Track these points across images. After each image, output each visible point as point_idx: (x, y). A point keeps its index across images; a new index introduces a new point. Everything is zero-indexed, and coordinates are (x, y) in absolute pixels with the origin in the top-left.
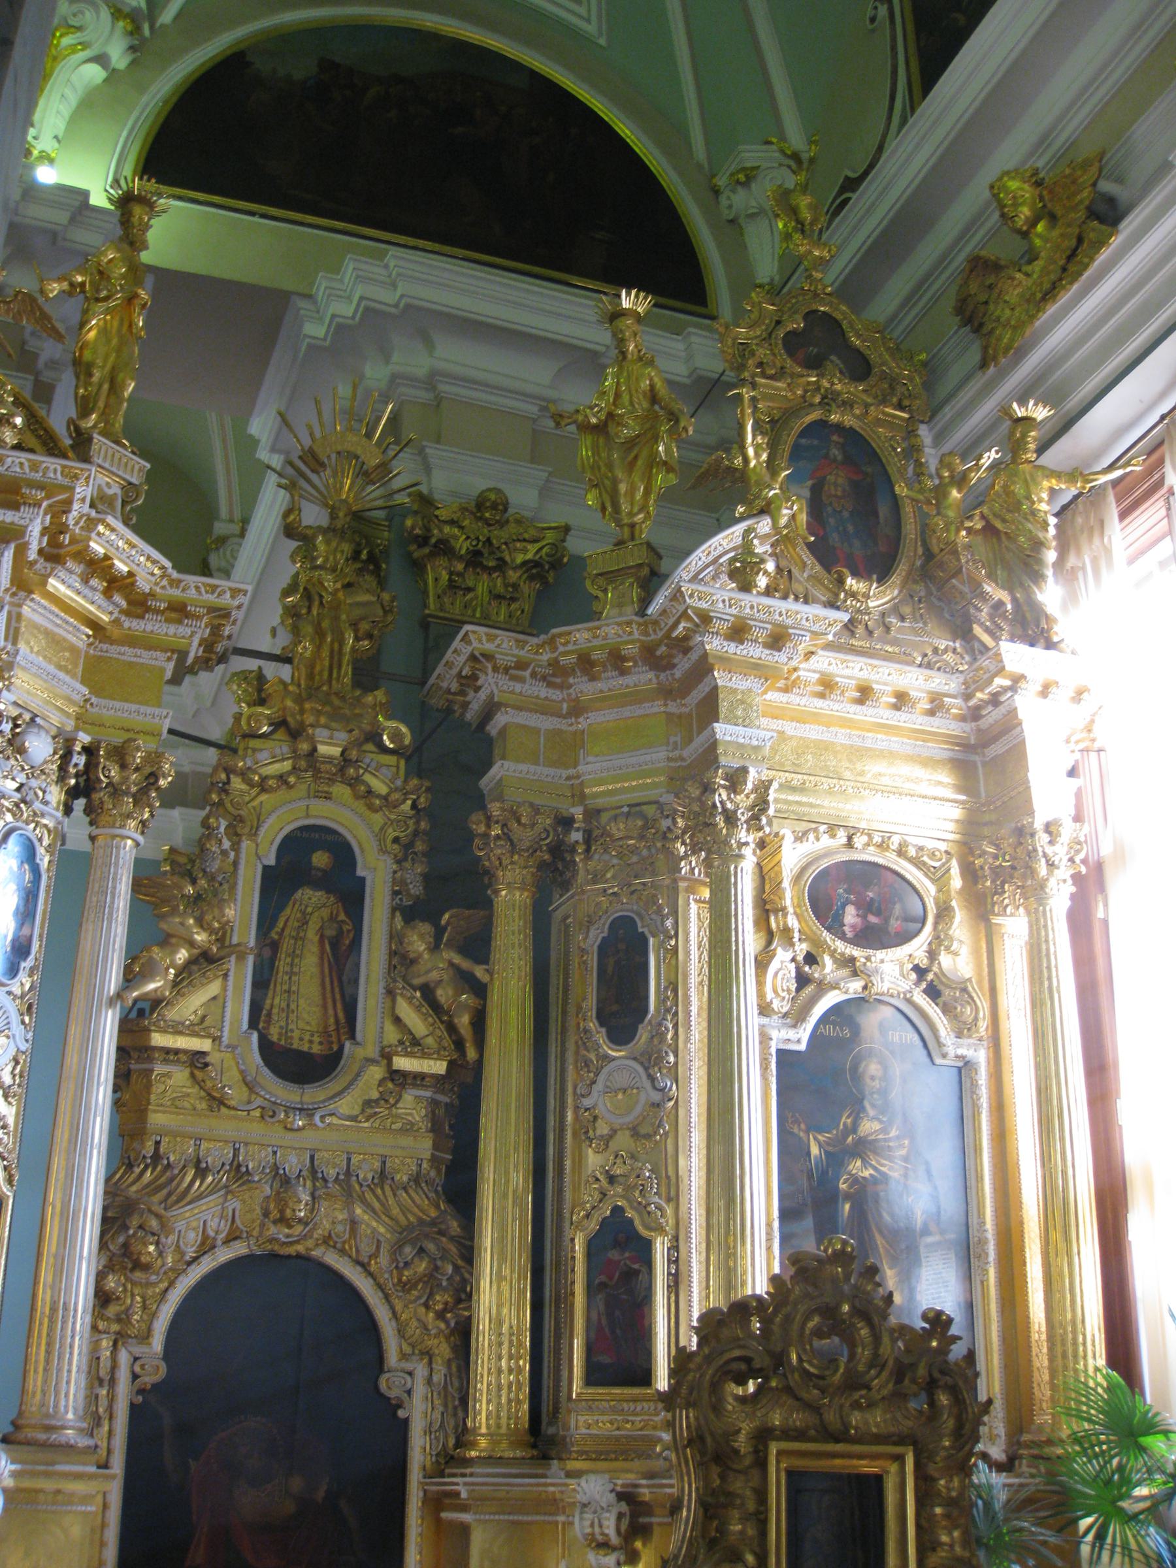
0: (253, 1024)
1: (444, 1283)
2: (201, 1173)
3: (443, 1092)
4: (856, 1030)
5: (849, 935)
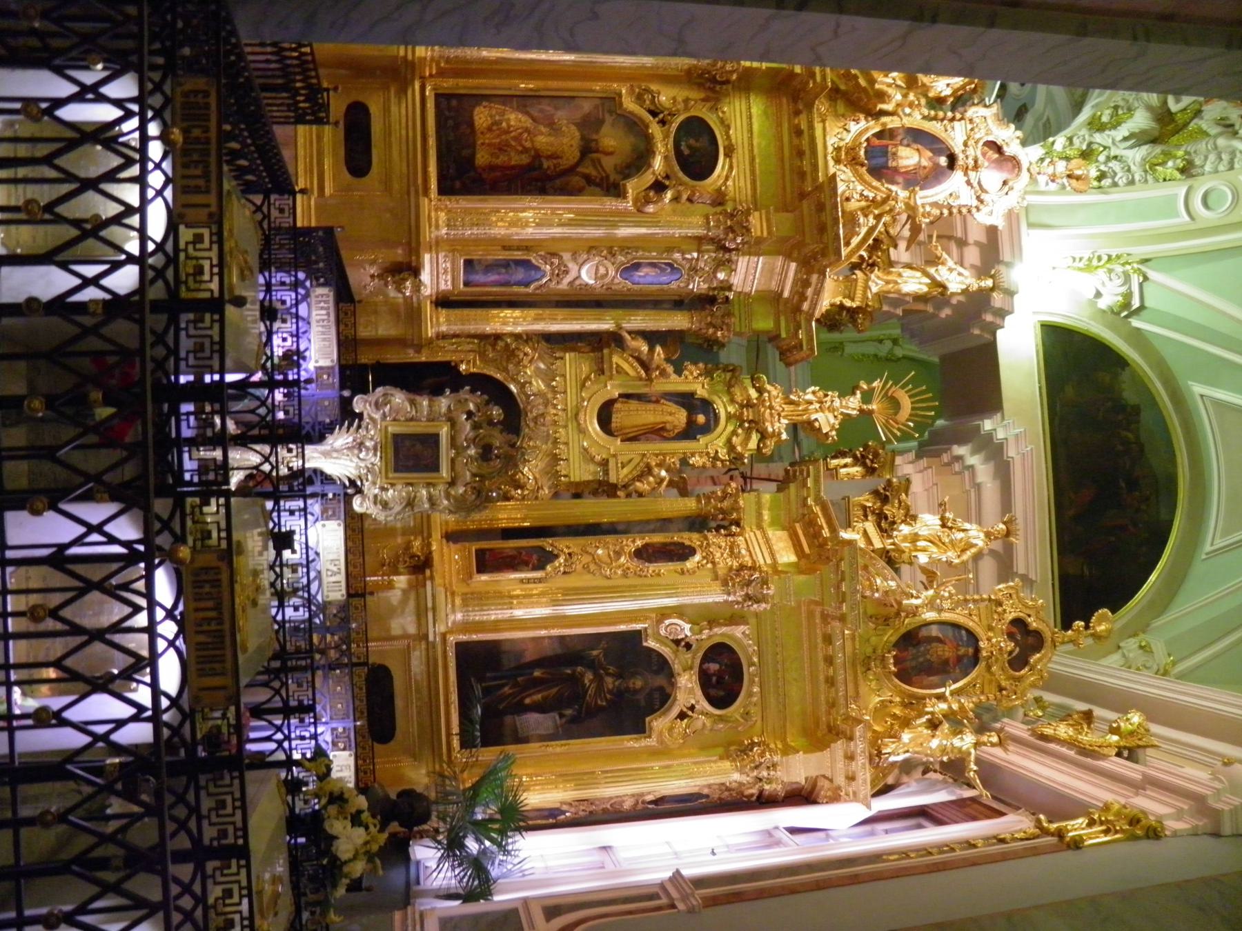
4: (657, 673)
5: (706, 666)
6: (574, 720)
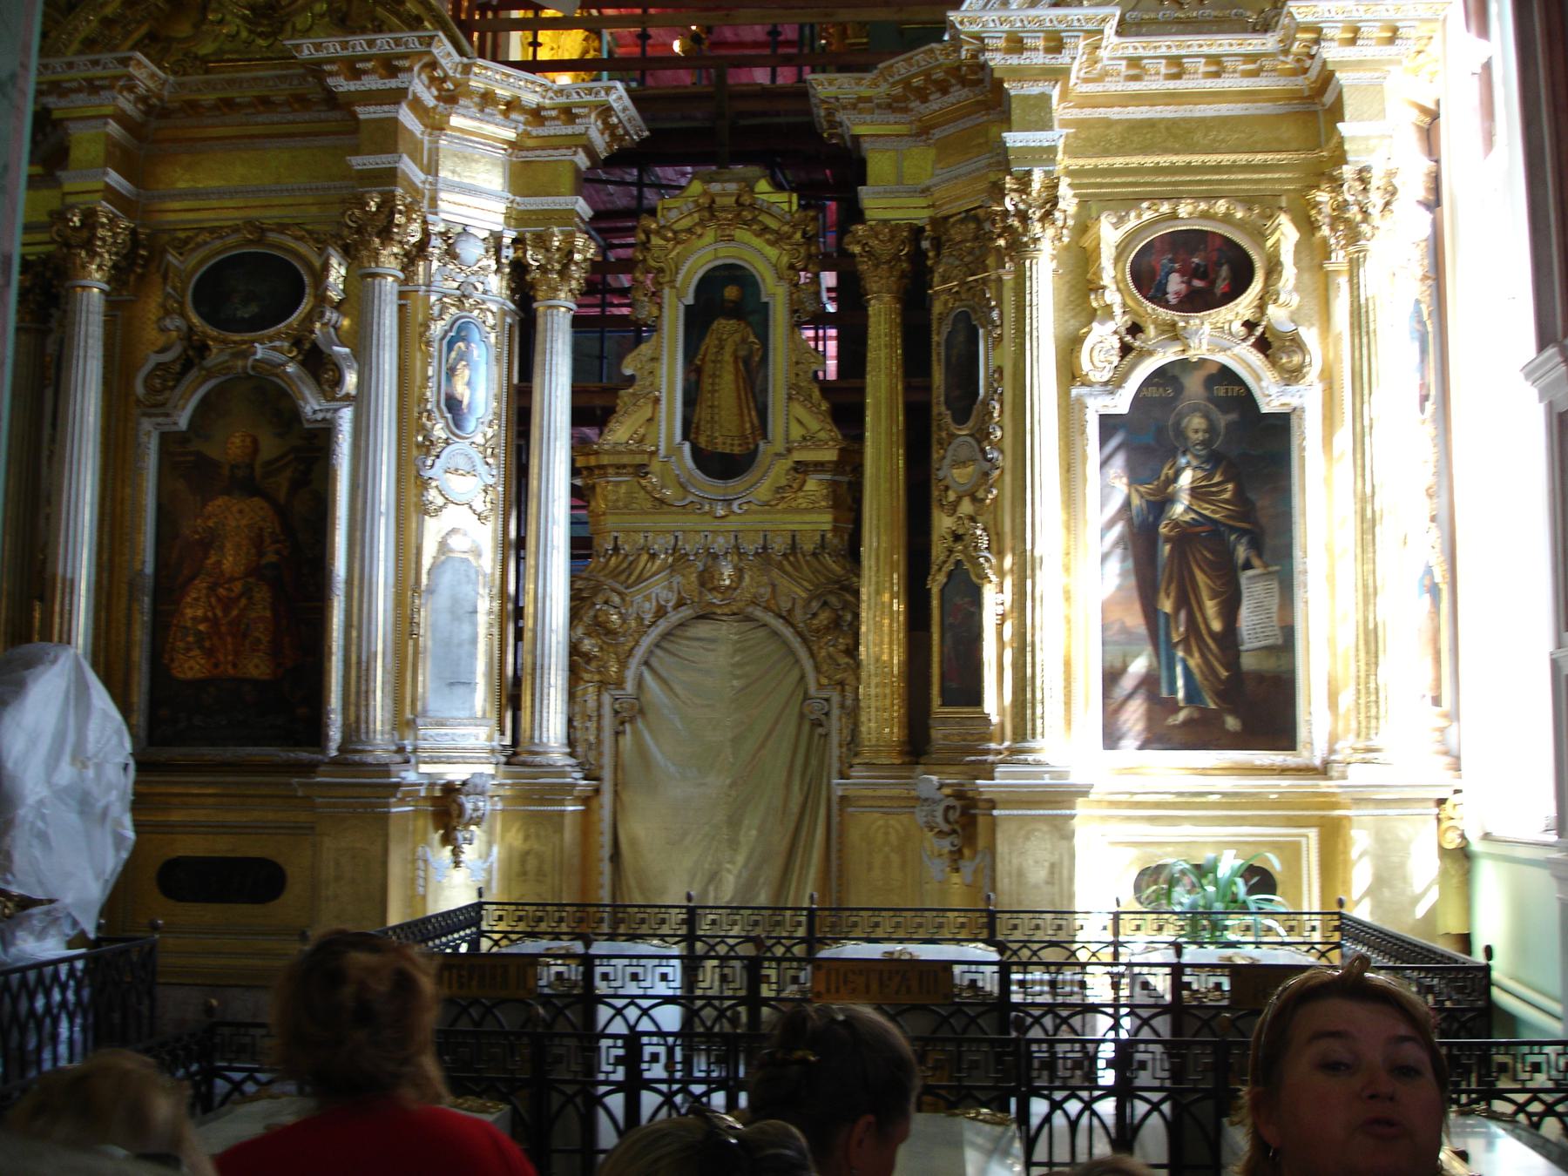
0: (685, 437)
1: (845, 628)
2: (653, 556)
3: (843, 473)
6: (1256, 545)
